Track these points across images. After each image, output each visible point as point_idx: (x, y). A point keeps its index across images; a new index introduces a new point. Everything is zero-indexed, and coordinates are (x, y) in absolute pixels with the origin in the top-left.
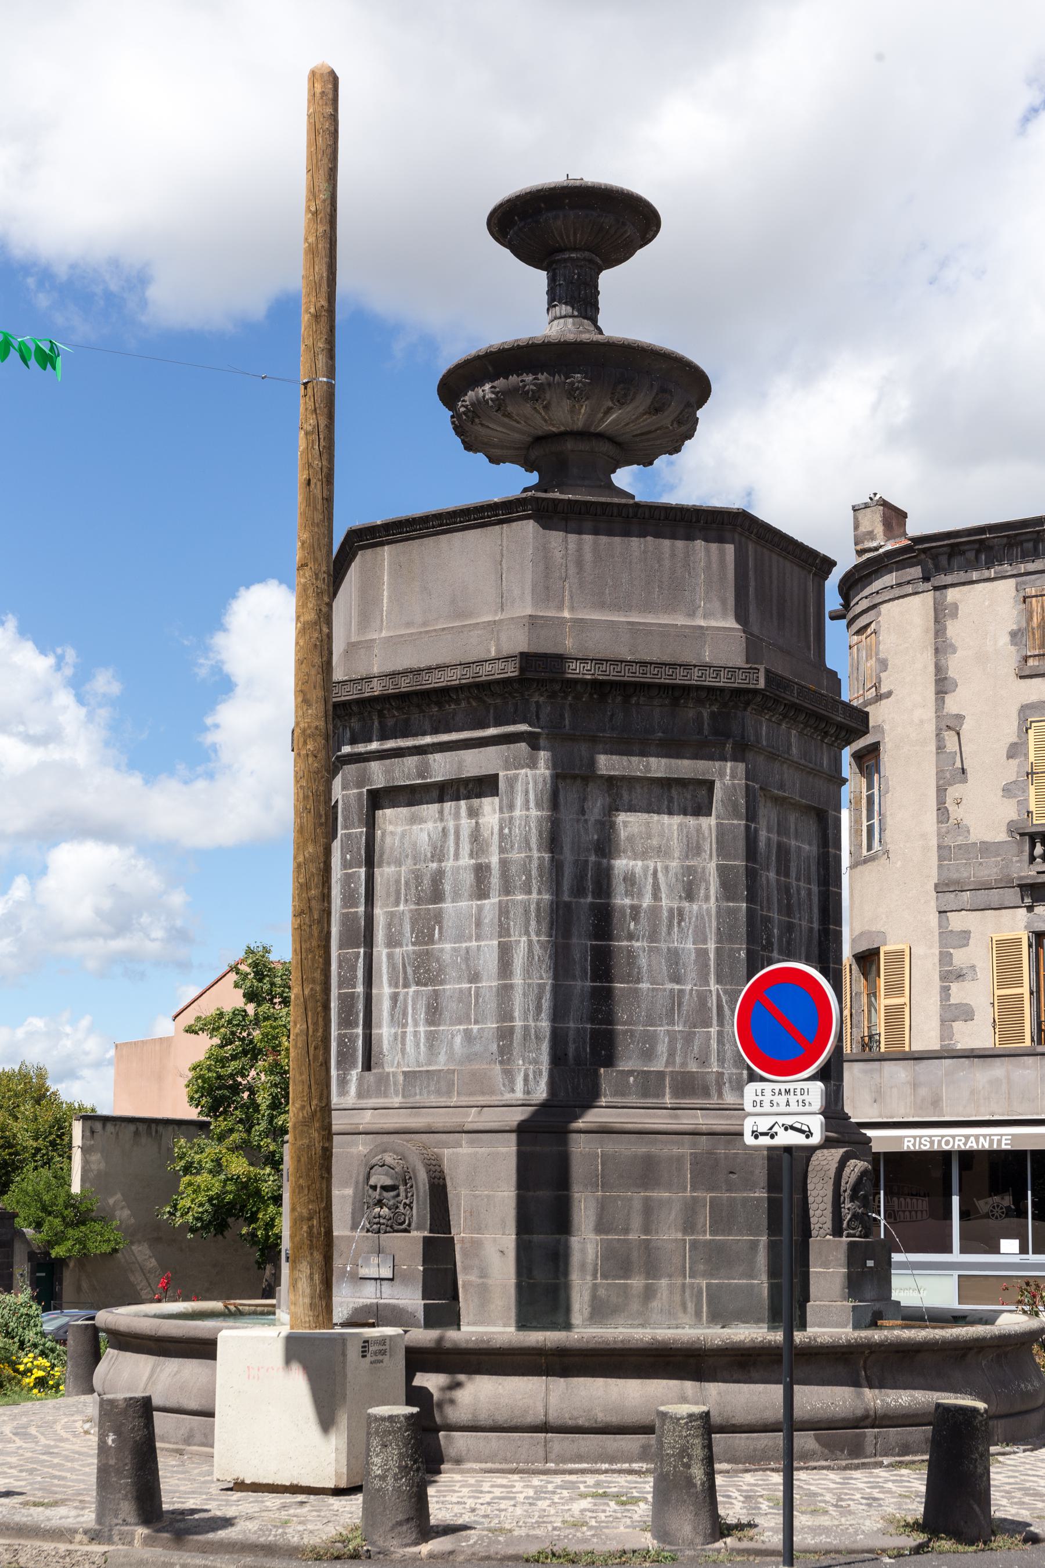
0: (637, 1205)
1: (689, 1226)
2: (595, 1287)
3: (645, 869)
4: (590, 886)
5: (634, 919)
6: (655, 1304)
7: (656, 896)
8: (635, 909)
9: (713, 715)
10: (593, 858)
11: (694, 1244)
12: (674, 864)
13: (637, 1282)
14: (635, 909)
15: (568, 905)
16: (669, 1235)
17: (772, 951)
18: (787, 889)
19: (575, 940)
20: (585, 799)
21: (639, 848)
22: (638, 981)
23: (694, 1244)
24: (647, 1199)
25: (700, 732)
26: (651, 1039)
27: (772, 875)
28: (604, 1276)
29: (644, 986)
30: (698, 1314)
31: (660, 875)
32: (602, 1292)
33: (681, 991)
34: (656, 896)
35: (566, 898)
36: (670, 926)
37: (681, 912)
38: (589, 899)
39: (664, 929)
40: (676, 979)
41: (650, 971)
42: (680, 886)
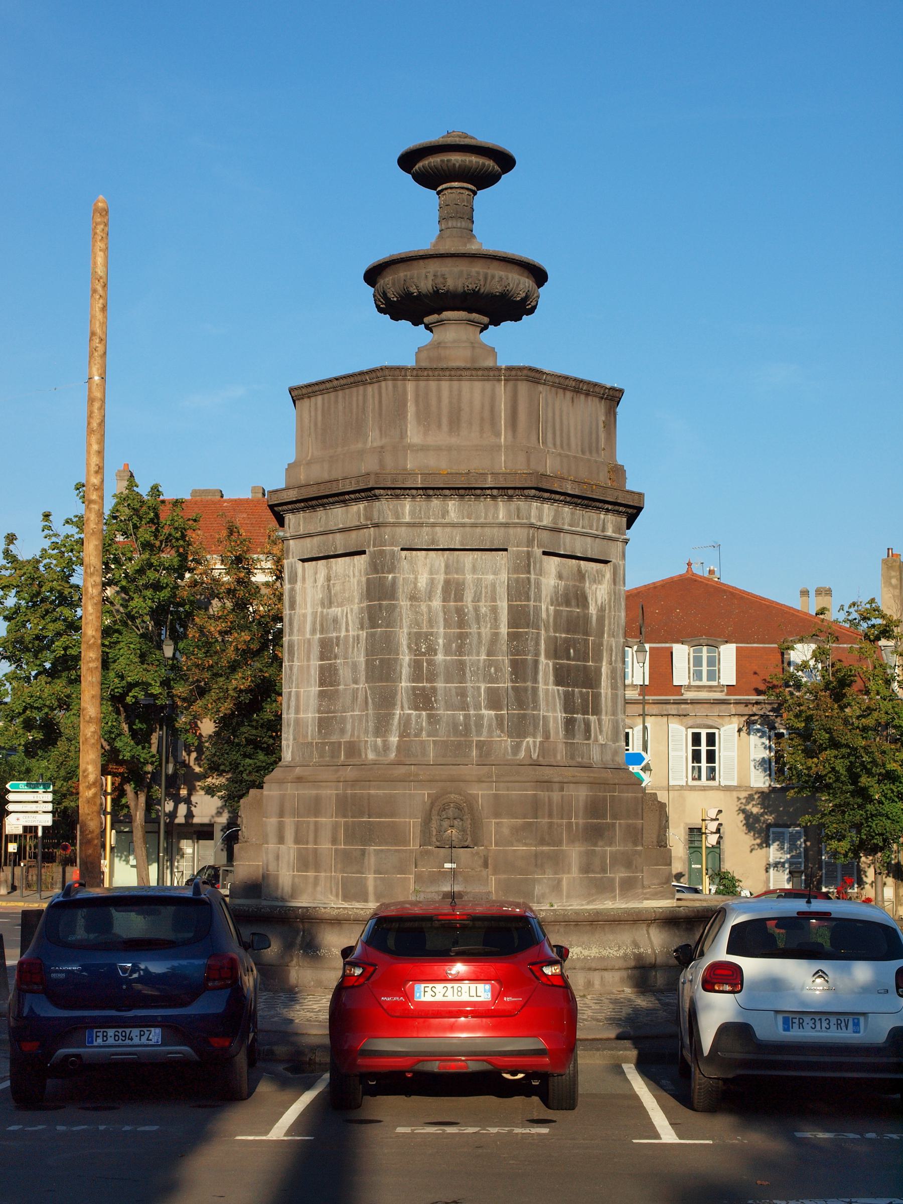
0: (312, 827)
1: (334, 841)
2: (294, 876)
3: (343, 611)
4: (318, 627)
5: (337, 645)
6: (319, 889)
7: (347, 630)
8: (338, 638)
9: (365, 508)
10: (320, 610)
11: (336, 850)
12: (356, 607)
13: (311, 874)
14: (338, 638)
15: (309, 640)
16: (325, 846)
17: (436, 654)
18: (460, 612)
19: (312, 662)
20: (316, 573)
21: (340, 600)
22: (339, 685)
23: (336, 850)
24: (316, 823)
25: (359, 520)
26: (343, 720)
27: (437, 603)
28: (298, 871)
29: (341, 687)
30: (337, 896)
31: (349, 615)
32: (296, 880)
33: (358, 689)
34: (347, 630)
35: (308, 636)
36: (353, 647)
37: (358, 636)
38: (318, 636)
39: (350, 650)
40: (356, 681)
41: (344, 678)
42: (357, 621)
